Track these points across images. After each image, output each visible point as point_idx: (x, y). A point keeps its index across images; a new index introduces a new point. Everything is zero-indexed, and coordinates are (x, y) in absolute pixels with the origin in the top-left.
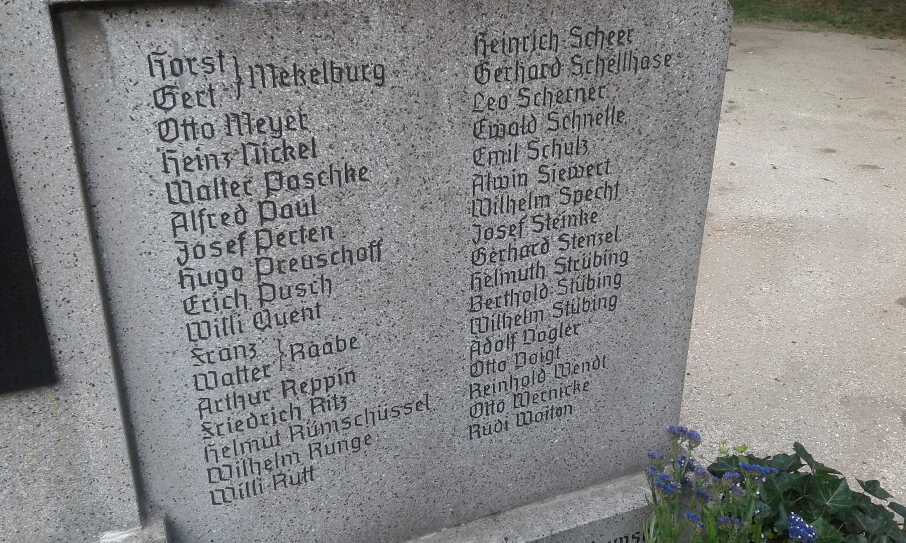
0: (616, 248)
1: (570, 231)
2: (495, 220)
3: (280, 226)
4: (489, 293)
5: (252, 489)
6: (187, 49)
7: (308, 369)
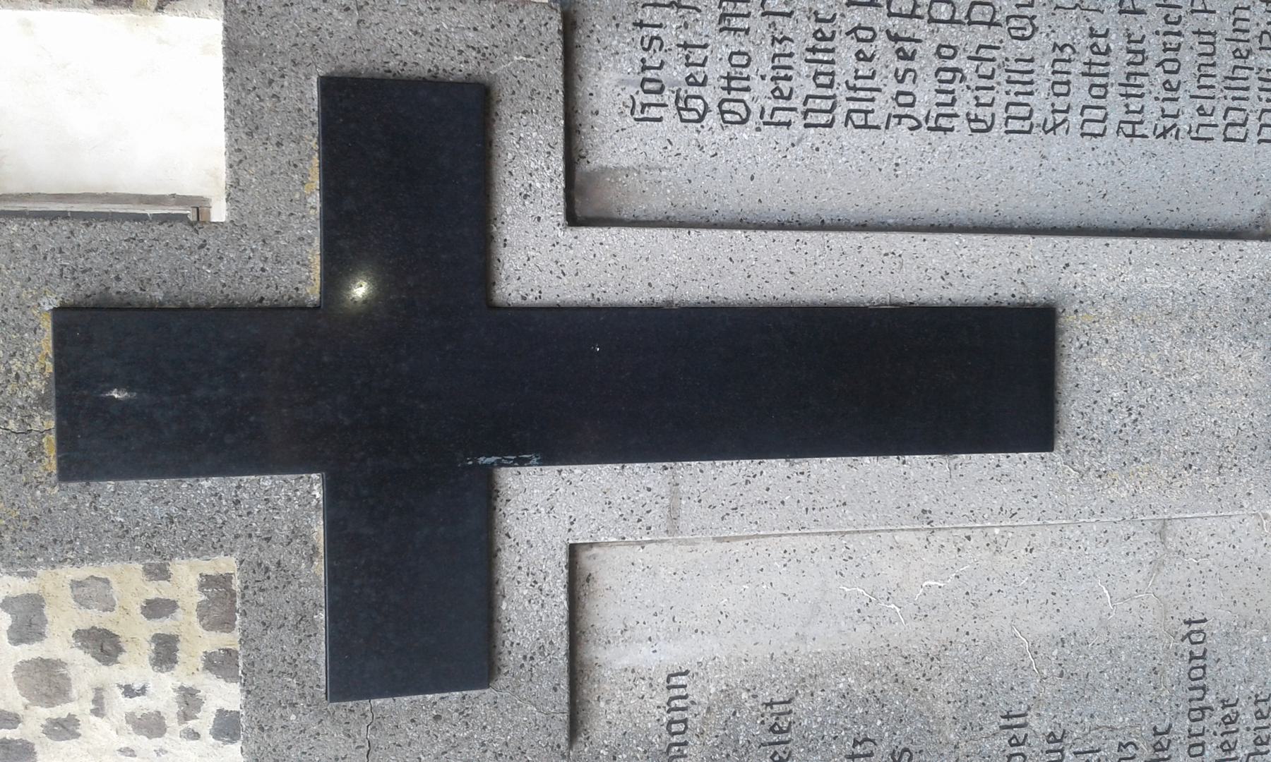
6: (628, 67)
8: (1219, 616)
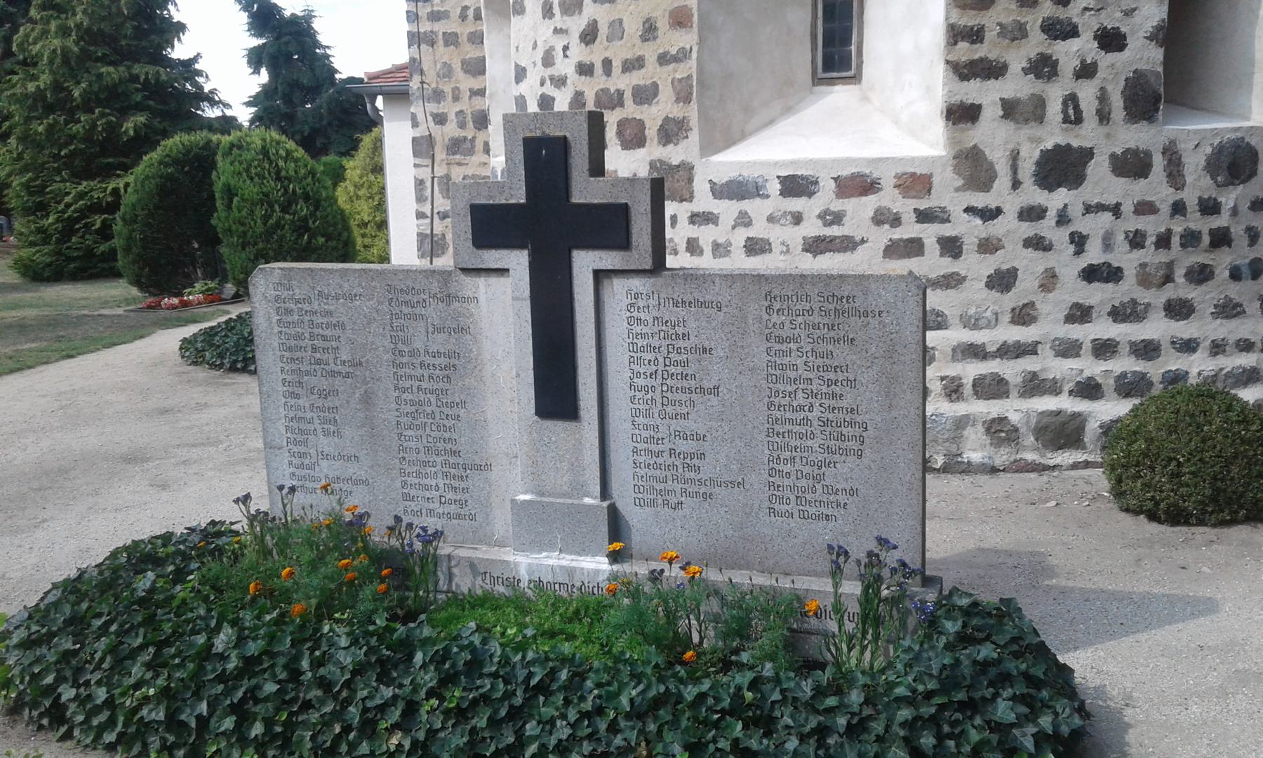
0: (859, 419)
1: (827, 403)
2: (780, 387)
3: (672, 369)
4: (778, 428)
5: (652, 503)
6: (641, 289)
7: (682, 446)
8: (493, 475)
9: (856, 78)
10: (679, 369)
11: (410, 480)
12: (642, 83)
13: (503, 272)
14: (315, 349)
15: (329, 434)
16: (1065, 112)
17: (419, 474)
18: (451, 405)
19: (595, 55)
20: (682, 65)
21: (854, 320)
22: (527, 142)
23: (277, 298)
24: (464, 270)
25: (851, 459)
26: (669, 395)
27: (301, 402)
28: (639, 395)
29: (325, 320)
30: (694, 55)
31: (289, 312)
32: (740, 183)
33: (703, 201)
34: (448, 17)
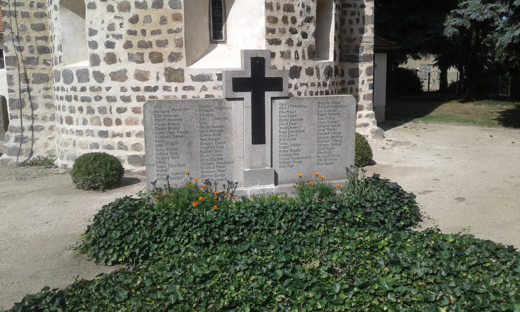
0: (340, 135)
1: (333, 131)
2: (321, 128)
3: (292, 126)
4: (320, 140)
5: (285, 166)
7: (294, 148)
8: (234, 165)
9: (225, 42)
10: (294, 126)
11: (204, 170)
12: (160, 39)
13: (242, 99)
14: (169, 128)
15: (174, 158)
16: (295, 56)
17: (208, 168)
18: (220, 143)
19: (133, 27)
20: (178, 34)
21: (340, 109)
22: (252, 59)
23: (155, 111)
24: (228, 99)
25: (338, 146)
26: (290, 133)
27: (163, 148)
28: (282, 134)
29: (174, 118)
30: (183, 31)
31: (160, 116)
32: (202, 76)
33: (188, 82)
34: (24, 5)
